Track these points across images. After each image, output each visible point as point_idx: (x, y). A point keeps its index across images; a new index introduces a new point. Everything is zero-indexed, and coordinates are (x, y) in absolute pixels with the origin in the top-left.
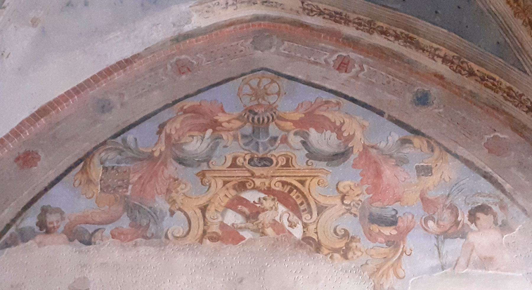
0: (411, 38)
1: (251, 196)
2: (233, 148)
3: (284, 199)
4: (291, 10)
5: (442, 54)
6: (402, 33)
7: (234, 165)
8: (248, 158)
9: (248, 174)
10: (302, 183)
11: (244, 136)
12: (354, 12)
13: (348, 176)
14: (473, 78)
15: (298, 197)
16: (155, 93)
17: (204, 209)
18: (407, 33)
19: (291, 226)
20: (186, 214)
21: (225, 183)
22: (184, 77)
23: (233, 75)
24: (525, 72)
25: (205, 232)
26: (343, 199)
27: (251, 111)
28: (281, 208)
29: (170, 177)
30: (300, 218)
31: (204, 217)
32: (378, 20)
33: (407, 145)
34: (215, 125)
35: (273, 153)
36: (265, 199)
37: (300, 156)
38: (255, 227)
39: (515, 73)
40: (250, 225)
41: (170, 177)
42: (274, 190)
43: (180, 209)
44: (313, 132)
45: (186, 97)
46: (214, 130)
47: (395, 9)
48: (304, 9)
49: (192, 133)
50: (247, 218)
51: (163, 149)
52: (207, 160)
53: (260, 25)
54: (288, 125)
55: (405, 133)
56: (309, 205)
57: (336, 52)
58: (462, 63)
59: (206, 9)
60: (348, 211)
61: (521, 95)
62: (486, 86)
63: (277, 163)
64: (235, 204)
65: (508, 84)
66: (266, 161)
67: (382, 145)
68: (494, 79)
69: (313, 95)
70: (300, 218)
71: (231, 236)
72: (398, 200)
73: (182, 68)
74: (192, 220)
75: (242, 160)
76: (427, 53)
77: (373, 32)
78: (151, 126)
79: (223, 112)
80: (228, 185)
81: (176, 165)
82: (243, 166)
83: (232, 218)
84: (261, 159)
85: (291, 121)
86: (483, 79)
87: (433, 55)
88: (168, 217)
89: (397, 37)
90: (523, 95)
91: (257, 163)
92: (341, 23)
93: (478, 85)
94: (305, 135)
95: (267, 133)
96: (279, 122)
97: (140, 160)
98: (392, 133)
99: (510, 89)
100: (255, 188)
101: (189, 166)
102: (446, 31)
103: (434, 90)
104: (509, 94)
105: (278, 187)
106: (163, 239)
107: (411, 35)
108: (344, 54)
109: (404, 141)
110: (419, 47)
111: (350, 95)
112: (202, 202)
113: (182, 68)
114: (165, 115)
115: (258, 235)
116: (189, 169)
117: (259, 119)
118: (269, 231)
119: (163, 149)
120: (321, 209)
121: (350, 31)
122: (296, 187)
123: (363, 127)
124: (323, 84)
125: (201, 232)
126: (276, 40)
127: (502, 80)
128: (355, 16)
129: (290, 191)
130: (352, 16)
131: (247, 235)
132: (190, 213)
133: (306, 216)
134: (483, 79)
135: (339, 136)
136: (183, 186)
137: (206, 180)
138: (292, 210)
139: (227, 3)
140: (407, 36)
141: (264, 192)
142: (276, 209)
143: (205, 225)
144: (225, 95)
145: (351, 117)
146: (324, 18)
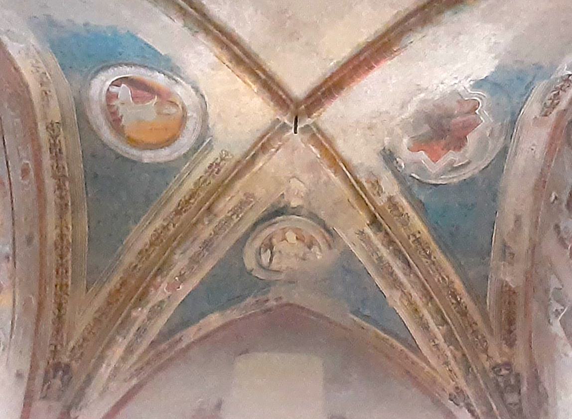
24: (87, 290)
65: (70, 283)
68: (67, 272)
86: (62, 265)
89: (61, 197)
92: (51, 153)
99: (67, 286)
104: (62, 287)
110: (61, 217)
121: (47, 161)
126: (18, 111)
127: (70, 278)
134: (62, 265)
139: (38, 67)
140: (66, 205)
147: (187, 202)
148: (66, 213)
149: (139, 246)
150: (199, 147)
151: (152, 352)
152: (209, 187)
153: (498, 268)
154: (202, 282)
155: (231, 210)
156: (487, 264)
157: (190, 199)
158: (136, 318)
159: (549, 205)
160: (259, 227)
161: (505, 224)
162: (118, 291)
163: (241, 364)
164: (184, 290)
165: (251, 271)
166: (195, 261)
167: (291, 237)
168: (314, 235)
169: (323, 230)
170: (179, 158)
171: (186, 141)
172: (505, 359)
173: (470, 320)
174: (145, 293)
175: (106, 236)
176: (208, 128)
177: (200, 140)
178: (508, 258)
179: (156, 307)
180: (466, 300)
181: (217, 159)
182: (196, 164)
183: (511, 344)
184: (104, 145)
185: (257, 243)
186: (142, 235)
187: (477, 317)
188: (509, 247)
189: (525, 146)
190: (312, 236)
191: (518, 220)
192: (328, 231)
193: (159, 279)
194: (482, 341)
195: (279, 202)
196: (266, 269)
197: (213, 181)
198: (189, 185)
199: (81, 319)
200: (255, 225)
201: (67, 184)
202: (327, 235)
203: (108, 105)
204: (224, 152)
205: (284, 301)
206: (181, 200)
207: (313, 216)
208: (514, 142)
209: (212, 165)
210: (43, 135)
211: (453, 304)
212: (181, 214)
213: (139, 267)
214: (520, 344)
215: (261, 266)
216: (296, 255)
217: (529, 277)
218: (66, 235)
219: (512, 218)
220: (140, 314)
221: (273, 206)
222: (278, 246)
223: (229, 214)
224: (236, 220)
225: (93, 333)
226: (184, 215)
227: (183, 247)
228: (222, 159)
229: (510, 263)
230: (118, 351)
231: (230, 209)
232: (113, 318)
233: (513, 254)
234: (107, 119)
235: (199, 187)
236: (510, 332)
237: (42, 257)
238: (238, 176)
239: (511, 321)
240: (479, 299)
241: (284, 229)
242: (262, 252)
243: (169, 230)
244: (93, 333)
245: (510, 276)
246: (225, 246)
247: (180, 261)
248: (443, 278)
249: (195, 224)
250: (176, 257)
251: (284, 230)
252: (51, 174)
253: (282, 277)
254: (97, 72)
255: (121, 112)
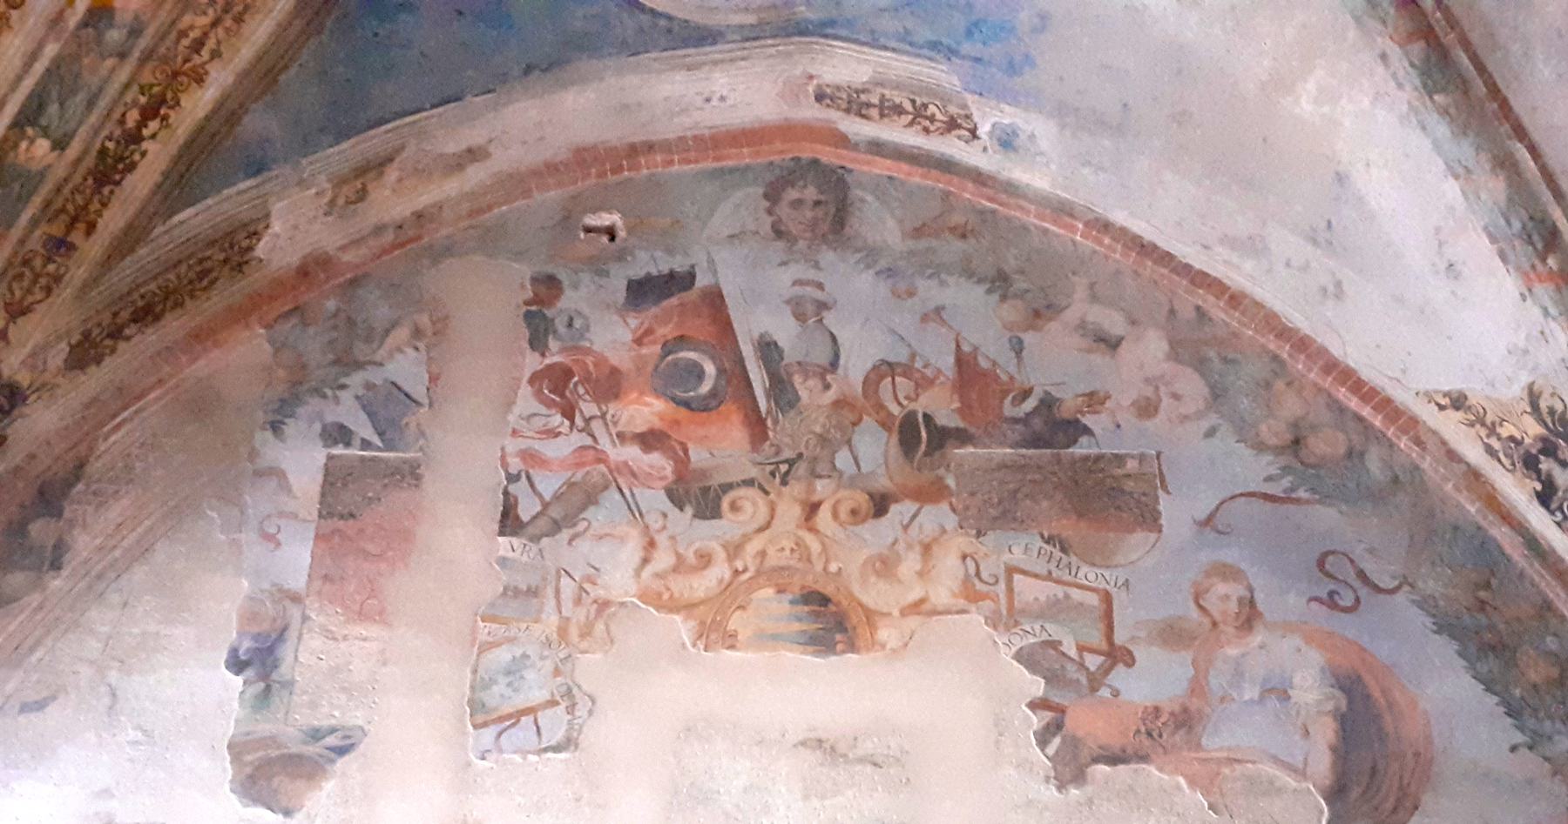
153: (302, 184)
156: (307, 145)
159: (567, 220)
161: (449, 132)
172: (24, 379)
173: (95, 206)
178: (347, 191)
180: (156, 156)
183: (85, 354)
187: (113, 220)
188: (381, 174)
189: (719, 81)
191: (474, 154)
194: (43, 281)
208: (730, 51)
211: (122, 121)
214: (95, 380)
217: (311, 270)
219: (473, 136)
229: (332, 203)
233: (362, 195)
236: (116, 334)
239: (147, 314)
240: (182, 184)
245: (294, 223)
248: (198, 46)
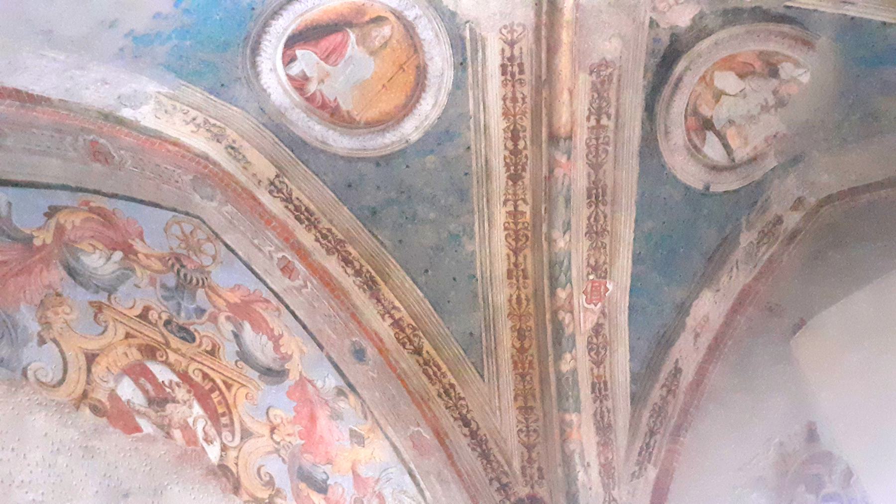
0: (375, 282)
1: (162, 374)
2: (141, 293)
3: (203, 398)
4: (254, 175)
5: (397, 316)
6: (368, 271)
7: (144, 316)
8: (165, 317)
9: (160, 339)
10: (229, 387)
11: (164, 286)
12: (331, 222)
13: (280, 403)
14: (416, 357)
15: (220, 403)
16: (54, 160)
17: (91, 358)
18: (374, 274)
19: (206, 440)
20: (62, 352)
21: (128, 336)
22: (98, 166)
23: (163, 204)
24: (482, 376)
25: (85, 395)
26: (273, 430)
27: (178, 259)
28: (197, 409)
29: (50, 286)
30: (220, 434)
31: (89, 370)
32: (351, 244)
33: (342, 398)
34: (129, 251)
35: (199, 328)
36: (178, 385)
37: (229, 350)
38: (159, 420)
39: (472, 373)
40: (152, 413)
41: (50, 286)
42: (192, 379)
43: (54, 341)
44: (247, 326)
45: (97, 192)
46: (126, 257)
47: (382, 243)
48: (272, 183)
49: (94, 242)
50: (151, 402)
51: (49, 241)
52: (111, 291)
53: (206, 167)
54: (221, 303)
55: (342, 383)
56: (232, 420)
57: (283, 251)
58: (415, 335)
59: (170, 108)
60: (277, 451)
61: (461, 399)
62: (425, 372)
63: (200, 345)
64: (138, 373)
65: (453, 381)
66: (187, 335)
67: (319, 384)
68: (440, 369)
69: (252, 284)
70: (220, 434)
71: (121, 417)
72: (329, 462)
73: (98, 154)
74: (69, 365)
75: (156, 316)
76: (381, 308)
77: (334, 254)
78: (43, 200)
79: (142, 240)
80: (131, 340)
81: (63, 273)
82: (156, 325)
83: (128, 390)
84: (182, 329)
85: (225, 300)
86: (426, 363)
87: (387, 312)
88: (34, 342)
89: (358, 273)
90: (464, 399)
91: (175, 330)
92: (301, 222)
93: (416, 367)
94: (239, 327)
95: (193, 297)
96: (210, 293)
97: (14, 239)
98: (330, 376)
99: (452, 386)
100: (166, 363)
101: (81, 284)
102: (421, 295)
103: (371, 352)
104: (447, 391)
105: (198, 378)
106: (19, 373)
107: (378, 279)
108: (290, 258)
109: (340, 392)
110: (377, 298)
111: (292, 308)
112: (92, 345)
113: (98, 154)
114: (62, 198)
115: (160, 434)
116: (80, 289)
117: (185, 275)
118: (177, 434)
119: (49, 241)
120: (246, 434)
121: (307, 238)
122: (220, 390)
123: (302, 351)
124: (264, 277)
125: (79, 391)
126: (219, 196)
127: (449, 374)
128: (328, 226)
129: (212, 390)
130: (324, 224)
131: (142, 422)
132: (69, 355)
133: (226, 434)
134: (426, 363)
135: (277, 348)
136: (68, 310)
137: (101, 317)
138: (210, 418)
139: (194, 119)
140: (372, 277)
141: (179, 374)
142: (191, 407)
143: (88, 383)
144: (151, 221)
145: (290, 334)
146: (287, 207)
147: (515, 152)
148: (379, 290)
149: (501, 267)
150: (464, 54)
151: (646, 414)
152: (528, 100)
154: (637, 259)
155: (590, 113)
157: (516, 145)
158: (574, 371)
160: (660, 108)
162: (522, 350)
163: (809, 347)
164: (619, 285)
165: (707, 188)
166: (597, 233)
167: (727, 81)
168: (763, 48)
169: (772, 26)
170: (451, 94)
171: (439, 59)
174: (558, 328)
175: (447, 279)
176: (454, 14)
177: (458, 44)
179: (595, 340)
181: (503, 50)
182: (481, 85)
184: (349, 160)
185: (678, 135)
186: (493, 249)
190: (761, 53)
192: (781, 19)
193: (562, 294)
195: (656, 40)
196: (732, 167)
197: (526, 90)
198: (497, 125)
199: (505, 423)
200: (650, 109)
201: (350, 249)
202: (786, 28)
203: (307, 99)
204: (504, 31)
205: (812, 200)
206: (505, 158)
207: (733, 16)
209: (503, 66)
210: (275, 206)
212: (521, 177)
213: (523, 296)
215: (715, 168)
216: (765, 108)
218: (400, 319)
220: (577, 361)
221: (651, 53)
222: (720, 113)
223: (593, 122)
224: (611, 124)
225: (535, 431)
226: (527, 175)
227: (559, 223)
228: (512, 44)
230: (584, 435)
231: (587, 113)
232: (541, 392)
234: (322, 120)
235: (514, 116)
237: (393, 367)
238: (552, 50)
241: (703, 78)
242: (699, 145)
243: (523, 213)
244: (535, 431)
246: (626, 177)
247: (573, 246)
249: (551, 171)
250: (561, 244)
251: (706, 80)
252: (323, 251)
253: (771, 163)
254: (254, 65)
255: (330, 95)
